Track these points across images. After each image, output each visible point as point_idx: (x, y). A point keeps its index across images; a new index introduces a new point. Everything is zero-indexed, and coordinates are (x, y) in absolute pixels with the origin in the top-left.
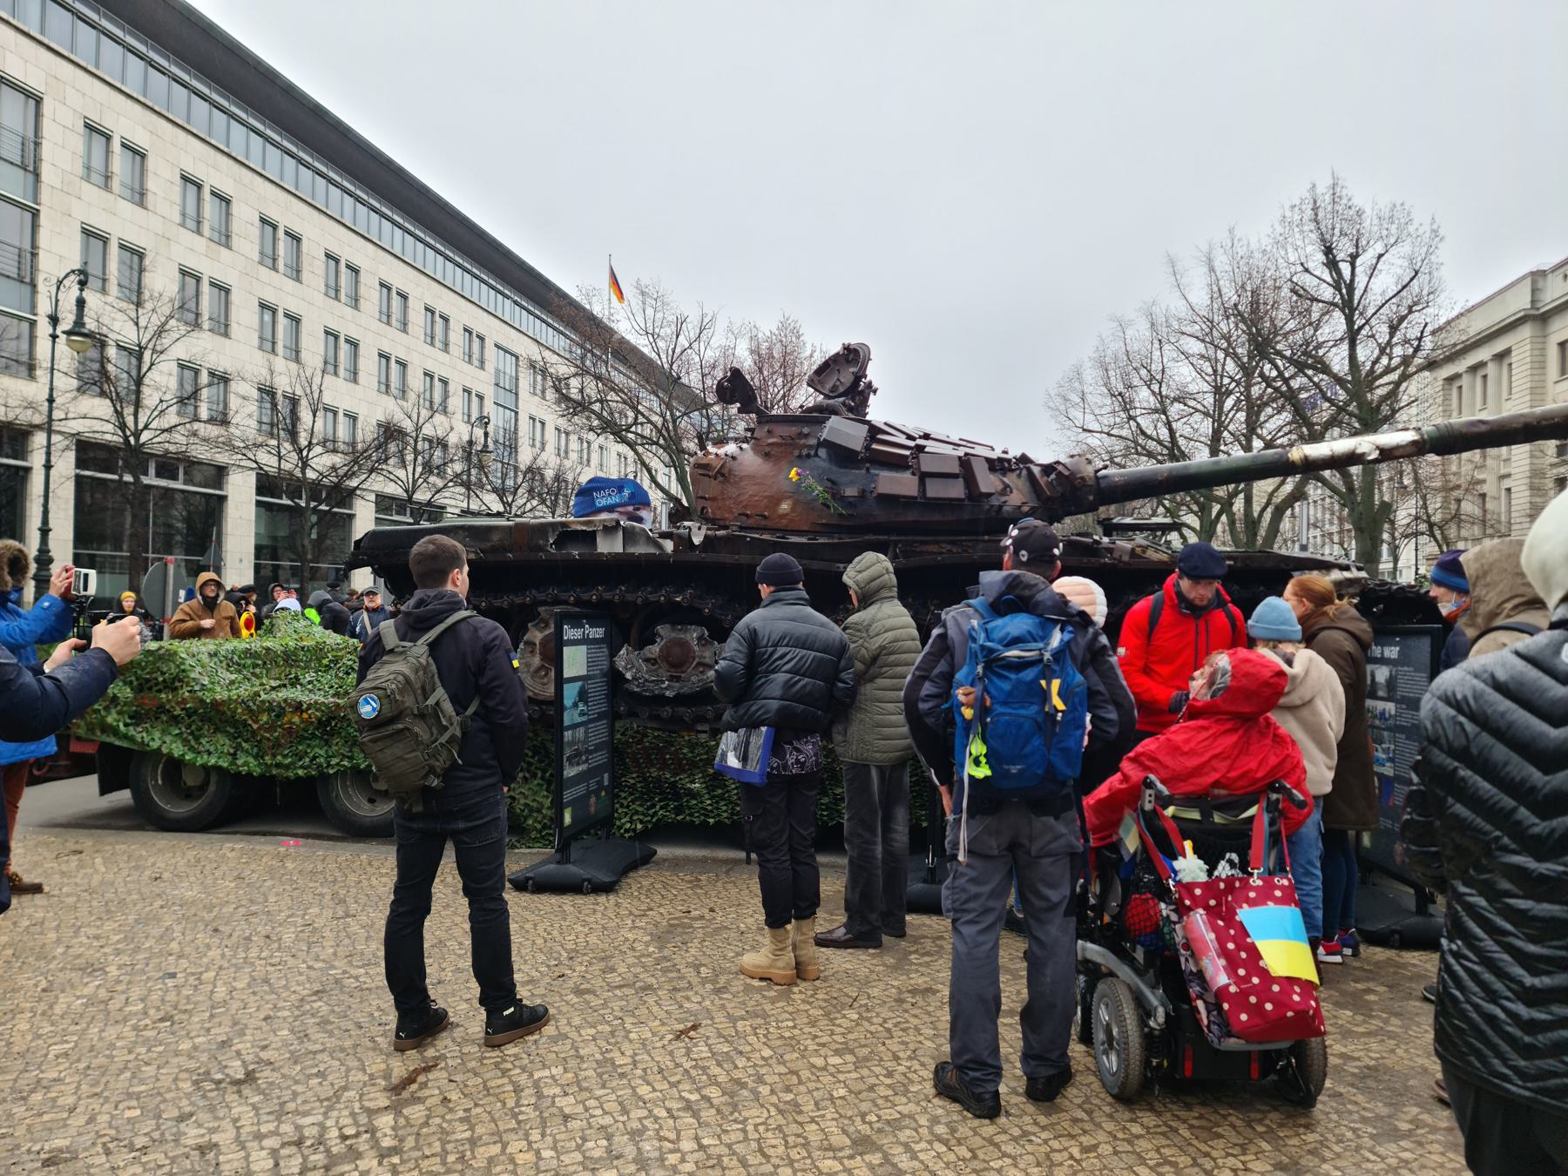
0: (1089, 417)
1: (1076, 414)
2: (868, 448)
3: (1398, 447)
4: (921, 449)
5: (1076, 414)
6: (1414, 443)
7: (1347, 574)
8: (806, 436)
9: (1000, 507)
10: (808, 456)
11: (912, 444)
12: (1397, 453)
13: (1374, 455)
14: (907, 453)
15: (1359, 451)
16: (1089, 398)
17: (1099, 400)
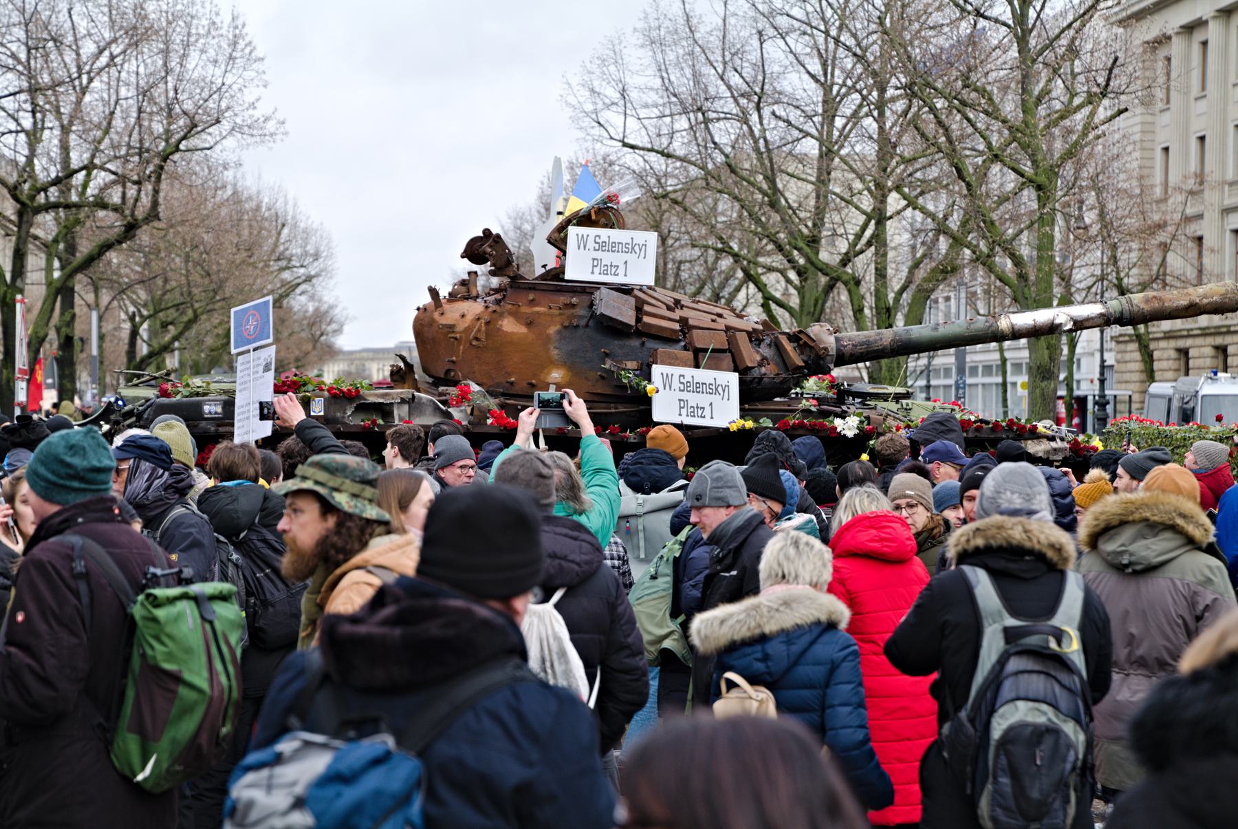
0: (632, 123)
1: (613, 118)
2: (638, 320)
3: (1088, 319)
4: (683, 321)
5: (613, 118)
6: (1102, 315)
7: (1053, 444)
8: (573, 306)
9: (761, 379)
10: (577, 326)
11: (678, 314)
12: (1087, 324)
13: (1069, 326)
14: (677, 326)
15: (1057, 321)
16: (633, 95)
17: (652, 97)
